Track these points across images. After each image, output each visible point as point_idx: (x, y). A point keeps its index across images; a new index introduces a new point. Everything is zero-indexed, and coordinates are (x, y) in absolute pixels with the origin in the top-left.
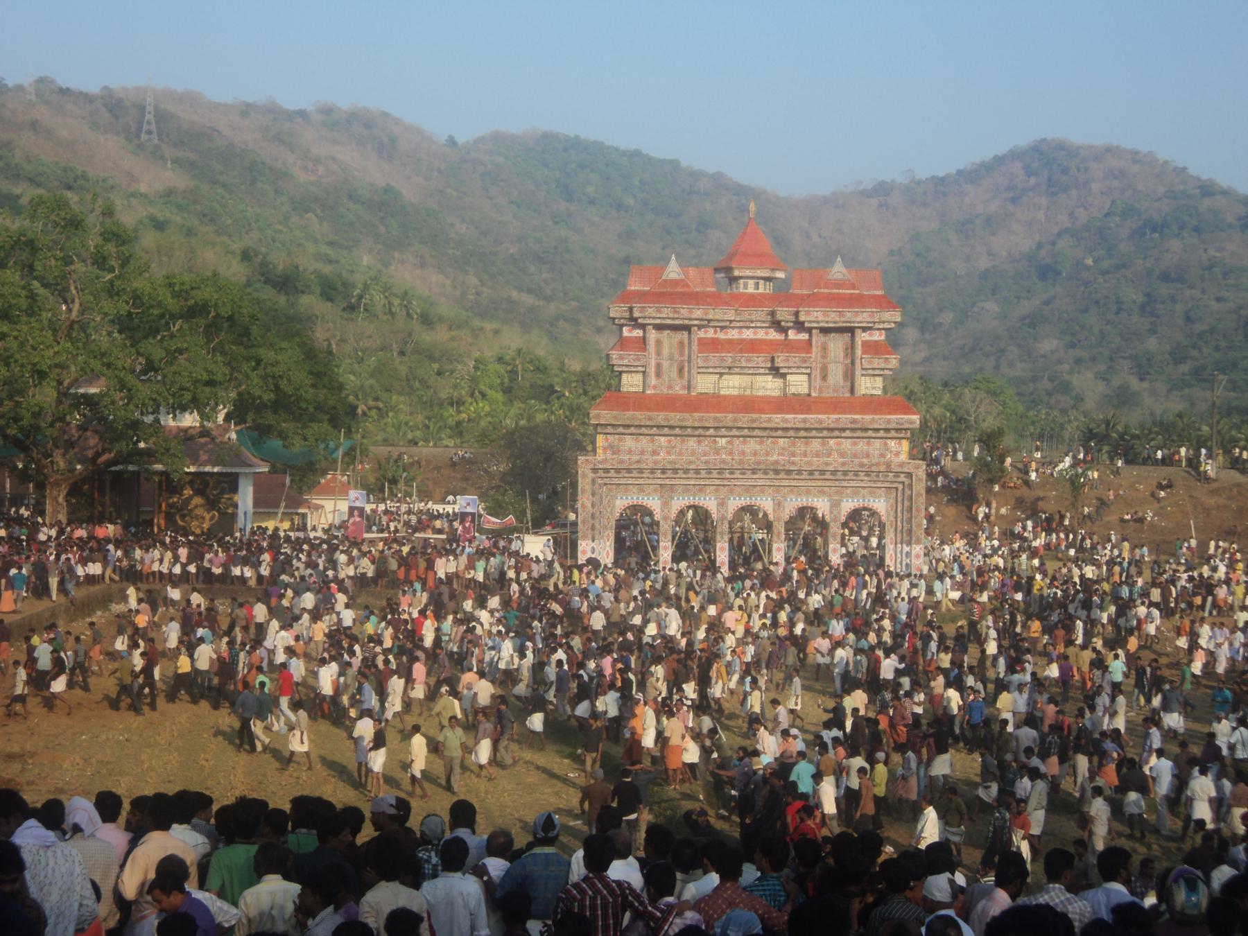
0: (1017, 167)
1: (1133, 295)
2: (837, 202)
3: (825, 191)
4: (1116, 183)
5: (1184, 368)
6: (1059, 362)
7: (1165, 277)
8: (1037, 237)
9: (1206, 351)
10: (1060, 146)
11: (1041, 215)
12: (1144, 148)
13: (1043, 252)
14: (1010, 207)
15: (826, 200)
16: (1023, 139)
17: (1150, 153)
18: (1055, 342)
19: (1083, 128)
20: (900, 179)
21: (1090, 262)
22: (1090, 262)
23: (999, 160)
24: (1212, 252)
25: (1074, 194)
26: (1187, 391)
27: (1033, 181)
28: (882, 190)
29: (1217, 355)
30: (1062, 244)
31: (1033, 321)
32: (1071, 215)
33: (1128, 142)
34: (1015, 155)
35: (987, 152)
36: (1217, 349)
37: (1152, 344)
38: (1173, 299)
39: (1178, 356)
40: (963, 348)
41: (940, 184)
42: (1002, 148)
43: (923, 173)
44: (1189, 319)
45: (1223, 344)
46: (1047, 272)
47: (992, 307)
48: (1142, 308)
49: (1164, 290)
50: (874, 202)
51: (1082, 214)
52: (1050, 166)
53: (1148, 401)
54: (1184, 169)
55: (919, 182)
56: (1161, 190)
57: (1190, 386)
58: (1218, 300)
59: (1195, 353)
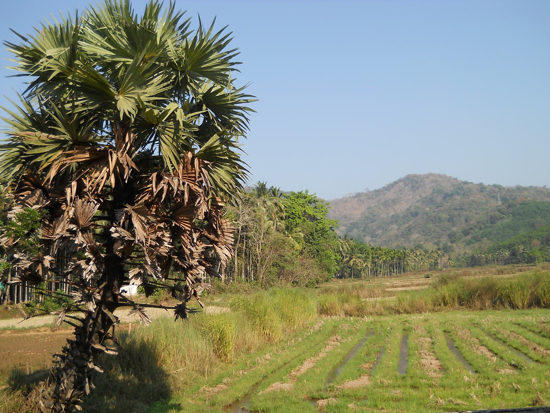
0: (402, 184)
1: (445, 216)
2: (345, 201)
3: (340, 197)
4: (434, 184)
5: (469, 237)
6: (420, 241)
7: (456, 209)
8: (410, 204)
9: (476, 230)
10: (415, 176)
11: (410, 197)
12: (442, 173)
13: (412, 208)
14: (400, 196)
15: (340, 200)
16: (403, 175)
17: (444, 175)
18: (418, 235)
19: (421, 169)
20: (364, 191)
21: (428, 209)
22: (428, 209)
23: (396, 183)
24: (471, 198)
25: (421, 189)
26: (472, 245)
27: (407, 187)
28: (358, 195)
29: (481, 231)
30: (417, 204)
31: (409, 230)
32: (420, 196)
33: (437, 171)
34: (400, 181)
35: (391, 181)
36: (481, 229)
37: (454, 229)
38: (460, 216)
39: (466, 233)
40: (385, 241)
41: (377, 192)
42: (396, 179)
43: (371, 189)
44: (466, 221)
45: (482, 226)
46: (415, 214)
47: (395, 227)
48: (449, 220)
49: (456, 213)
50: (356, 199)
51: (424, 195)
52: (412, 182)
53: (457, 250)
54: (456, 179)
55: (370, 192)
56: (449, 185)
57: (472, 243)
58: (476, 214)
59: (472, 231)
